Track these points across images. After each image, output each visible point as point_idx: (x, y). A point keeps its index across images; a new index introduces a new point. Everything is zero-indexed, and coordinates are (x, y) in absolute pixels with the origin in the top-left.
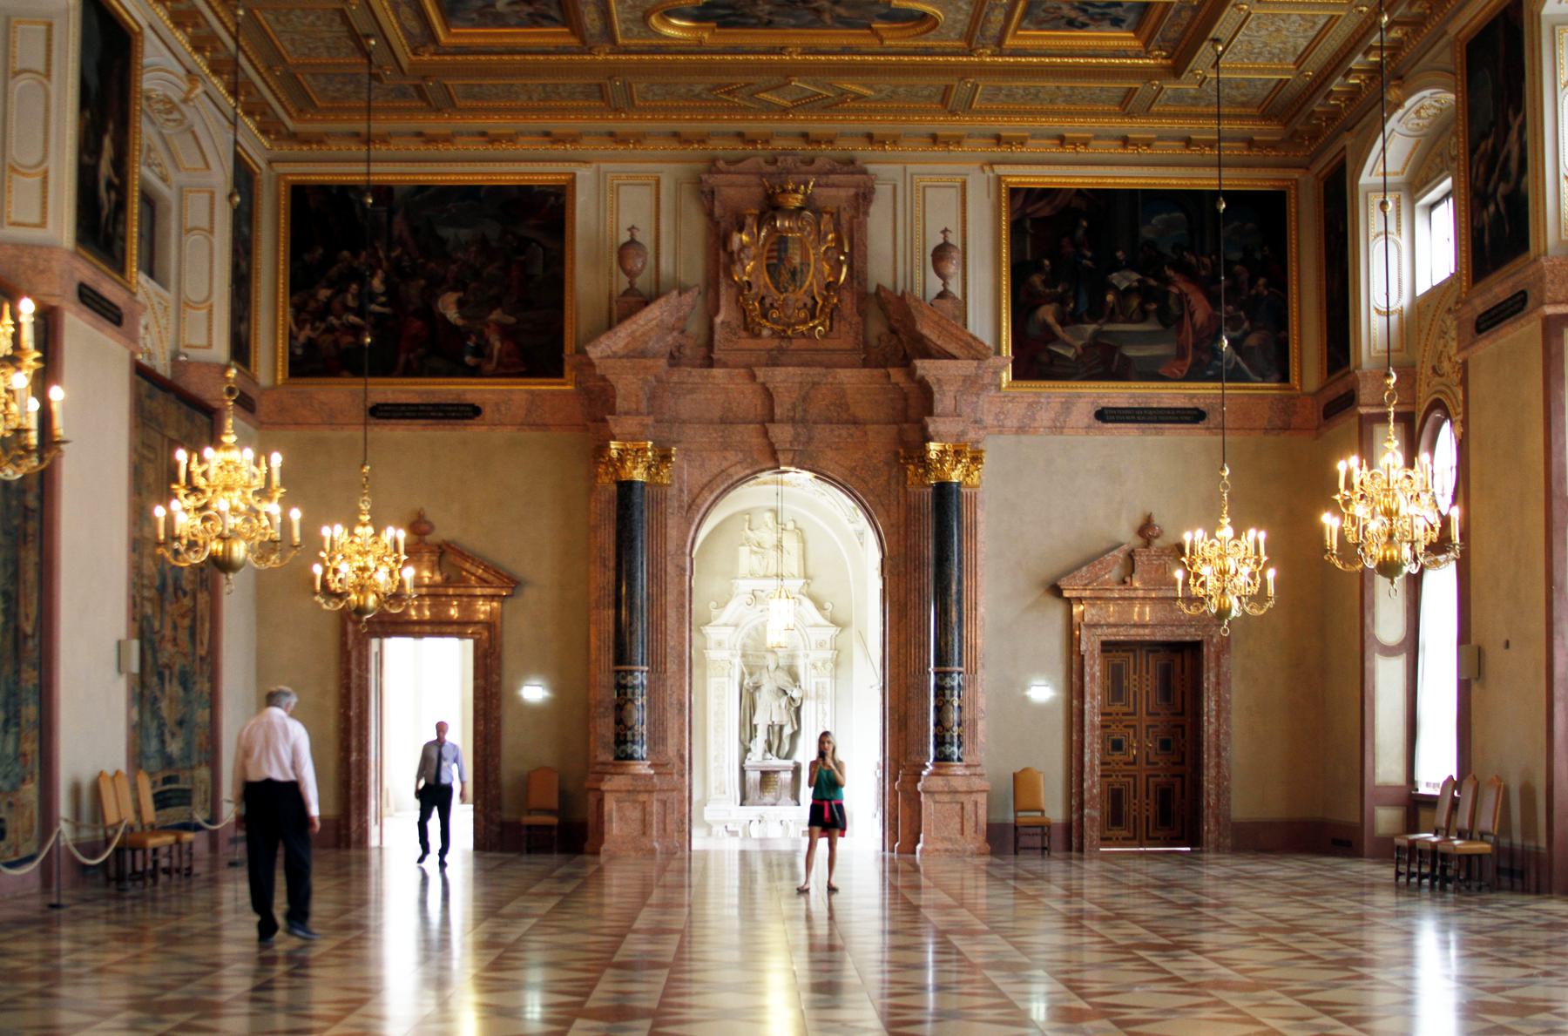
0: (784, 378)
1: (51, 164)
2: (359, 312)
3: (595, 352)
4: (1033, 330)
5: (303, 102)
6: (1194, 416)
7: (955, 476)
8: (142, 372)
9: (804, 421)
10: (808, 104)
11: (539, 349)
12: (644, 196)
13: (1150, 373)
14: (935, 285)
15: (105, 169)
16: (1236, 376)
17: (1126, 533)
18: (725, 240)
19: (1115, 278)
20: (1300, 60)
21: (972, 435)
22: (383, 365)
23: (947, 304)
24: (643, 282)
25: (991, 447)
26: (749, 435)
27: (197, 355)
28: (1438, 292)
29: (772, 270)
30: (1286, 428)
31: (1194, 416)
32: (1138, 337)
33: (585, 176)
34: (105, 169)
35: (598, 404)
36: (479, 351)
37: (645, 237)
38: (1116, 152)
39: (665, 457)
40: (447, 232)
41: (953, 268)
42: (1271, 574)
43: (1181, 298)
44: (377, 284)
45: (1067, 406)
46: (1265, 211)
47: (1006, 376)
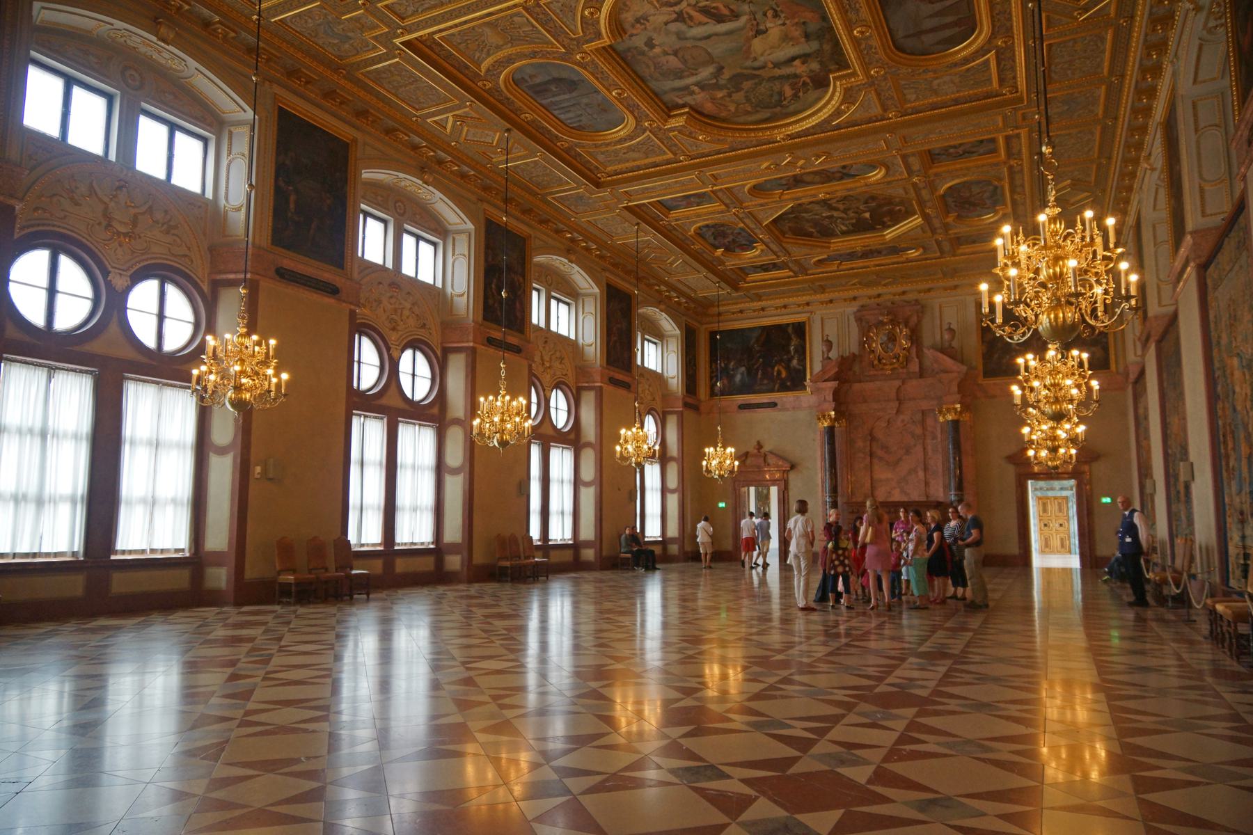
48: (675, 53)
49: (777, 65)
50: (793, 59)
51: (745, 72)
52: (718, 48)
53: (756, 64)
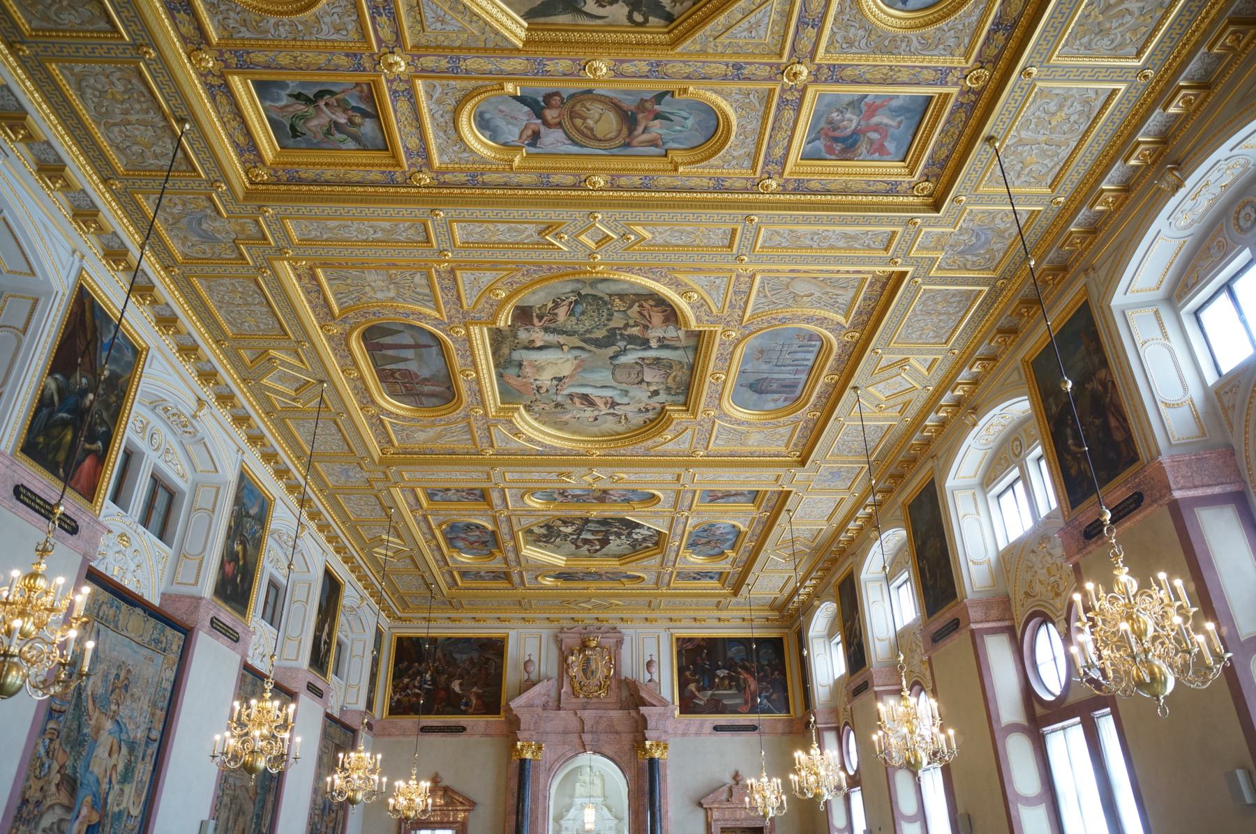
0: (588, 715)
1: (303, 636)
2: (420, 688)
3: (513, 705)
4: (687, 694)
5: (405, 606)
6: (753, 728)
7: (657, 755)
8: (328, 716)
9: (596, 732)
10: (597, 607)
11: (491, 704)
12: (536, 642)
13: (734, 710)
14: (648, 677)
15: (324, 636)
16: (768, 711)
17: (729, 780)
18: (566, 659)
19: (718, 672)
20: (781, 590)
21: (663, 738)
22: (427, 710)
23: (652, 684)
24: (534, 676)
25: (672, 742)
26: (574, 738)
27: (350, 707)
28: (841, 677)
29: (584, 671)
30: (791, 733)
31: (753, 728)
32: (729, 696)
33: (512, 634)
34: (324, 636)
35: (514, 724)
36: (467, 704)
37: (535, 658)
38: (716, 623)
39: (540, 748)
40: (456, 656)
41: (654, 669)
42: (784, 798)
43: (745, 680)
44: (428, 676)
45: (702, 725)
46: (776, 645)
47: (677, 712)
48: (642, 381)
49: (560, 346)
50: (540, 348)
51: (593, 348)
52: (604, 376)
53: (577, 353)
